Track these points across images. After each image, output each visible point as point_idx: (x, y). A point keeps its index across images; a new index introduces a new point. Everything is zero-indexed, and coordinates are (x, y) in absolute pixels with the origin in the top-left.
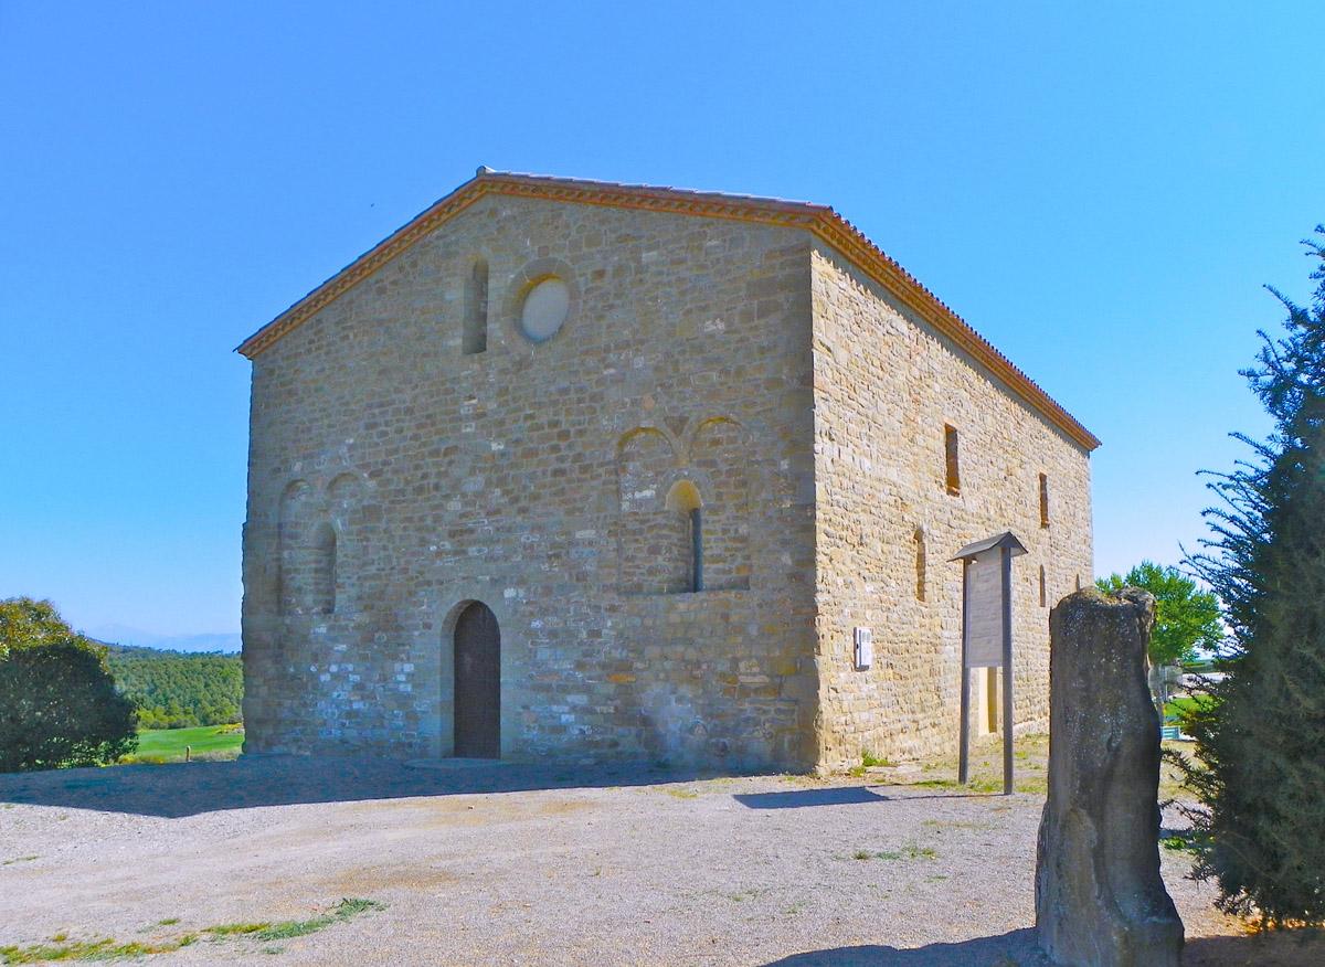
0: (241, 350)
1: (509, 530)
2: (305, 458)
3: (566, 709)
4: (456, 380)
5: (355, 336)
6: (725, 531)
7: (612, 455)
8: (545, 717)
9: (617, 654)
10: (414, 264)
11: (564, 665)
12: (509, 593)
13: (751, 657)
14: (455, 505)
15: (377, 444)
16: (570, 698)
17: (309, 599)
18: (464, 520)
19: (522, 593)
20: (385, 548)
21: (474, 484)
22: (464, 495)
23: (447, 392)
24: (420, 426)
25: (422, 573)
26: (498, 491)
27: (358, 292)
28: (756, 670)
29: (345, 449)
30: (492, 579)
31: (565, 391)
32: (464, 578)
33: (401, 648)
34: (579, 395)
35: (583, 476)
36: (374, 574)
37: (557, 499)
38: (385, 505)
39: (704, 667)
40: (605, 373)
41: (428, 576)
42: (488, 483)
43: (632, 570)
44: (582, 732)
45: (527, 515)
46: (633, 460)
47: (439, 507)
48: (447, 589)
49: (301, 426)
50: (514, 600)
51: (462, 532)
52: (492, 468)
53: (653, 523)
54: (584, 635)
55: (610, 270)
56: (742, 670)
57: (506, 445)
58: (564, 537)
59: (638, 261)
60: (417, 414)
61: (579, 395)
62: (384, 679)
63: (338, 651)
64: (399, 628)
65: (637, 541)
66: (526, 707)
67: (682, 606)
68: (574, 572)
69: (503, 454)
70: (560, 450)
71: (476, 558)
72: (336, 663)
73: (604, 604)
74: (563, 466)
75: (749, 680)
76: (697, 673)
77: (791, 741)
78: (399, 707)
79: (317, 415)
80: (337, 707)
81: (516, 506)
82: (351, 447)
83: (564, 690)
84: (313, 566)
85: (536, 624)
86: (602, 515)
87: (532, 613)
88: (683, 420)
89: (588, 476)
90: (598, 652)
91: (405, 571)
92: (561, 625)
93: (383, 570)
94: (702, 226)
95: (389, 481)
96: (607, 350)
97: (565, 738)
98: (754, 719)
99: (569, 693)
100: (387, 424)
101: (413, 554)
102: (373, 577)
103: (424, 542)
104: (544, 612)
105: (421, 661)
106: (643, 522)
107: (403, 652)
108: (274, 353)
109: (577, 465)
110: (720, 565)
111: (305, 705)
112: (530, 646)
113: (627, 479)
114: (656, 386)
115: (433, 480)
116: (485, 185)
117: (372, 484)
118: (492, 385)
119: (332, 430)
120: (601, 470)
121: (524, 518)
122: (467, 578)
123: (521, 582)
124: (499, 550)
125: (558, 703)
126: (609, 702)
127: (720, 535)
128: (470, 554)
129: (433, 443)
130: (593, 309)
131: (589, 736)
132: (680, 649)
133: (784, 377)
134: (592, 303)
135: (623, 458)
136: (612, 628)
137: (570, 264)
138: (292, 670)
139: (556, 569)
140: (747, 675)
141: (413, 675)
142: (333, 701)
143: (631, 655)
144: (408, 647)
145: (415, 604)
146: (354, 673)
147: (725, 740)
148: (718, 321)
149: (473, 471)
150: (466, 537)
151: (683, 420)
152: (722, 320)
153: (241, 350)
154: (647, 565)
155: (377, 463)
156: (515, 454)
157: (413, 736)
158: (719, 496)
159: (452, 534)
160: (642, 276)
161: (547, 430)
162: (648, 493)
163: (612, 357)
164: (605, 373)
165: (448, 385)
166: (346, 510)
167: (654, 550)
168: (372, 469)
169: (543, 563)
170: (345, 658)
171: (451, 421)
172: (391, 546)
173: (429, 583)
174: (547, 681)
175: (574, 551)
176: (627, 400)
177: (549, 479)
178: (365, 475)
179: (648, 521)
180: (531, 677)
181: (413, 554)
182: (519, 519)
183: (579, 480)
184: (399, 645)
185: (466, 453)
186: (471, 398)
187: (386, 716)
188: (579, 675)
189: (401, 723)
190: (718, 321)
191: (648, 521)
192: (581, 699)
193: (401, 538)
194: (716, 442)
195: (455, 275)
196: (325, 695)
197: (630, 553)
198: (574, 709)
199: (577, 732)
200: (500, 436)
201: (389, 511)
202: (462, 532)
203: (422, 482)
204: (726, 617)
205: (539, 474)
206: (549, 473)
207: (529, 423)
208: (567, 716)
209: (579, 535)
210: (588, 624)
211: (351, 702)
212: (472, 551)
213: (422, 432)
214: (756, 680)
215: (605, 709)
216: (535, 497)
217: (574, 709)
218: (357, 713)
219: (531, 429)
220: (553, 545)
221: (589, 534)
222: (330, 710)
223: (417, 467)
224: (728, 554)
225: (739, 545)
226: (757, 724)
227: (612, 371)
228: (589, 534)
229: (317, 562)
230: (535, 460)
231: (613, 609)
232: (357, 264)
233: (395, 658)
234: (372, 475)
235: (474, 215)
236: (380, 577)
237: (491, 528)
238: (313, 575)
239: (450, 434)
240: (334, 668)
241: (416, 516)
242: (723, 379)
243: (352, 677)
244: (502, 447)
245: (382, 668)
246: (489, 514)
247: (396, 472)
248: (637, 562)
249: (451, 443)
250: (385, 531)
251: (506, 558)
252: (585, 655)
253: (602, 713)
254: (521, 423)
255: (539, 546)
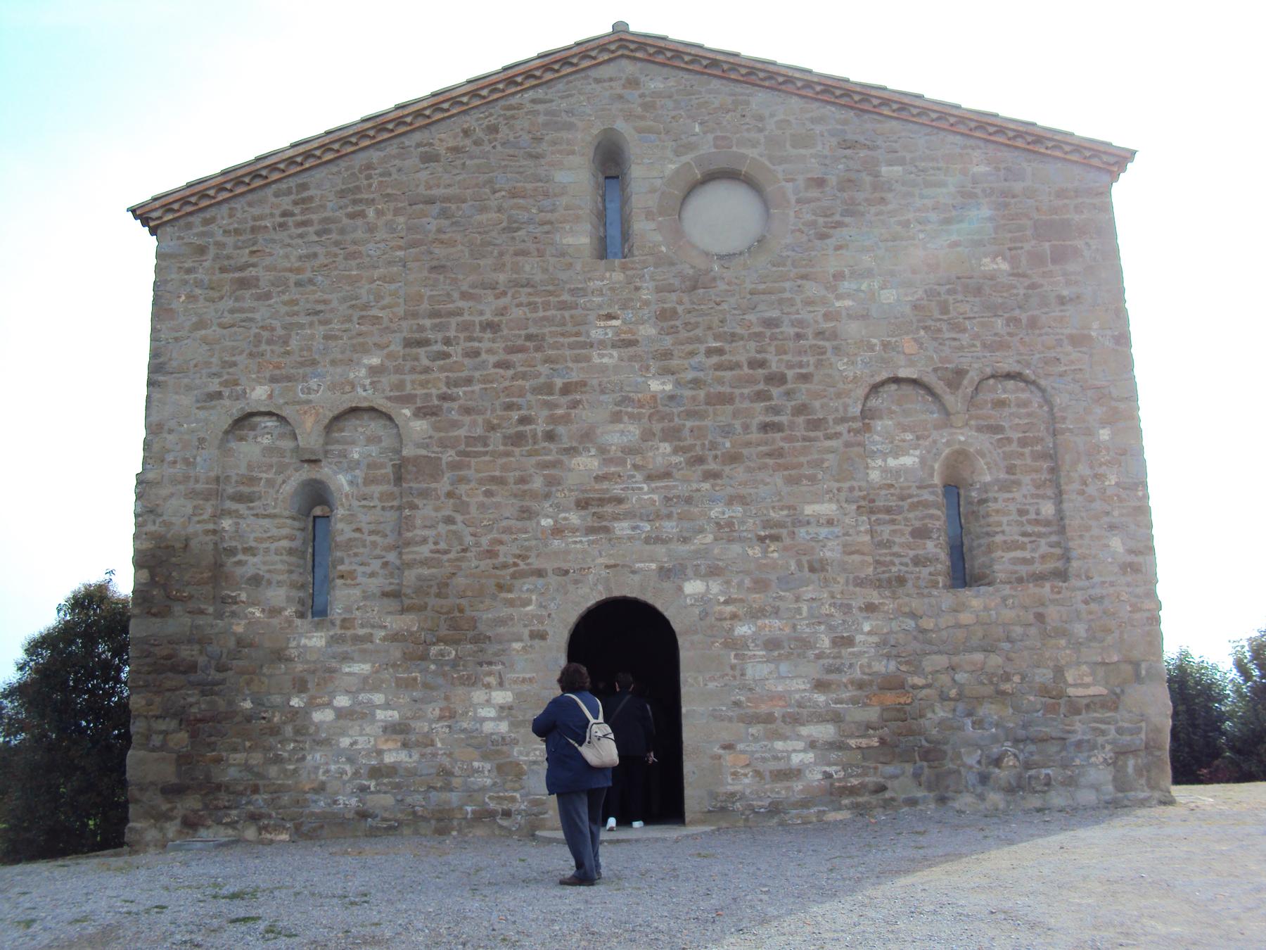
0: (142, 214)
1: (689, 500)
2: (273, 380)
3: (800, 745)
4: (582, 292)
5: (380, 213)
6: (1021, 512)
7: (856, 410)
8: (764, 760)
9: (880, 667)
10: (493, 129)
11: (792, 683)
12: (693, 587)
13: (1078, 664)
14: (587, 463)
15: (427, 370)
16: (804, 731)
17: (277, 595)
18: (605, 485)
19: (715, 587)
20: (449, 520)
21: (618, 436)
22: (602, 450)
23: (563, 306)
24: (512, 350)
25: (523, 557)
26: (666, 447)
27: (382, 154)
28: (1088, 680)
29: (363, 372)
30: (661, 568)
31: (770, 323)
32: (607, 567)
33: (486, 668)
34: (797, 330)
35: (812, 434)
36: (426, 559)
37: (770, 461)
38: (449, 456)
39: (1016, 679)
40: (837, 304)
41: (536, 563)
42: (647, 435)
43: (888, 559)
44: (828, 776)
45: (719, 482)
46: (881, 418)
47: (553, 465)
48: (576, 582)
49: (266, 334)
50: (702, 599)
51: (602, 502)
52: (650, 416)
53: (915, 500)
54: (825, 643)
55: (833, 180)
56: (1070, 680)
57: (678, 384)
58: (785, 512)
59: (877, 175)
60: (505, 332)
61: (797, 330)
62: (449, 715)
63: (349, 674)
64: (480, 639)
65: (893, 522)
66: (729, 747)
67: (976, 603)
68: (805, 559)
69: (672, 398)
70: (770, 398)
71: (630, 538)
72: (347, 692)
73: (856, 603)
74: (776, 419)
75: (1080, 692)
76: (1007, 687)
77: (1135, 766)
78: (485, 757)
79: (303, 320)
80: (350, 760)
81: (700, 469)
82: (373, 371)
83: (795, 720)
84: (285, 543)
85: (743, 630)
86: (846, 485)
87: (734, 616)
88: (960, 373)
89: (820, 434)
90: (851, 665)
91: (491, 554)
92: (787, 630)
93: (446, 552)
94: (965, 147)
95: (455, 425)
96: (839, 276)
97: (798, 786)
98: (1088, 741)
99: (803, 725)
100: (447, 342)
101: (507, 530)
102: (424, 563)
103: (527, 514)
104: (756, 614)
105: (525, 687)
106: (903, 498)
107: (490, 674)
108: (877, 214)
109: (801, 420)
110: (1019, 554)
111: (278, 760)
112: (734, 661)
113: (876, 440)
114: (918, 329)
115: (540, 427)
116: (623, 46)
117: (420, 426)
118: (647, 303)
119: (332, 343)
120: (839, 428)
121: (713, 486)
122: (615, 566)
123: (713, 572)
124: (670, 527)
125: (784, 738)
126: (871, 732)
127: (1015, 516)
128: (618, 532)
129: (539, 375)
130: (813, 224)
131: (839, 780)
132: (978, 657)
133: (1094, 334)
134: (809, 217)
135: (867, 415)
136: (870, 633)
137: (767, 163)
138: (248, 705)
139: (776, 555)
140: (1075, 685)
141: (510, 708)
142: (340, 753)
143: (903, 668)
144: (500, 667)
145: (511, 603)
146: (387, 706)
147: (1049, 771)
148: (999, 259)
149: (616, 418)
150: (609, 509)
151: (960, 373)
152: (1004, 259)
153: (142, 214)
154: (912, 553)
155: (428, 396)
156: (694, 398)
157: (513, 799)
158: (1010, 470)
159: (582, 504)
160: (883, 195)
161: (746, 370)
162: (909, 461)
163: (846, 286)
164: (837, 304)
165: (566, 297)
166: (358, 463)
167: (921, 533)
168: (419, 404)
169: (752, 547)
170: (367, 684)
171: (572, 346)
172: (459, 518)
173: (540, 573)
174: (764, 709)
175: (803, 530)
176: (874, 341)
177: (755, 436)
178: (407, 412)
179: (910, 496)
180: (737, 704)
181: (507, 530)
182: (706, 486)
183: (805, 439)
184: (481, 664)
185: (603, 392)
186: (610, 317)
187: (457, 771)
188: (820, 698)
189: (489, 782)
190: (999, 259)
191: (910, 496)
192: (826, 732)
193: (482, 506)
194: (1001, 404)
195: (573, 153)
196: (326, 742)
197: (886, 536)
198: (812, 745)
199: (820, 776)
200: (666, 371)
201: (454, 466)
202: (602, 502)
203: (521, 428)
204: (1040, 617)
205: (739, 429)
206: (754, 428)
207: (715, 359)
208: (801, 756)
209: (809, 510)
210: (831, 628)
211: (380, 752)
212: (622, 528)
213: (516, 358)
214: (1092, 691)
215: (864, 742)
216: (734, 458)
217: (812, 745)
218: (392, 770)
219: (719, 367)
220: (767, 524)
221: (827, 508)
222: (333, 767)
223: (509, 407)
224: (1026, 540)
225: (1043, 530)
226: (1094, 747)
227: (848, 303)
228: (827, 508)
229: (291, 538)
230: (729, 408)
231: (870, 608)
232: (392, 116)
233: (472, 682)
234: (420, 413)
235: (598, 81)
236: (439, 564)
237: (656, 497)
238: (285, 558)
239: (570, 365)
240: (342, 701)
241: (511, 476)
242: (1012, 329)
243: (380, 715)
244: (669, 387)
245: (447, 698)
246: (649, 478)
247: (467, 411)
248: (896, 549)
249: (575, 377)
250: (450, 495)
251: (685, 540)
252: (829, 670)
253: (859, 748)
254: (701, 358)
255: (743, 523)
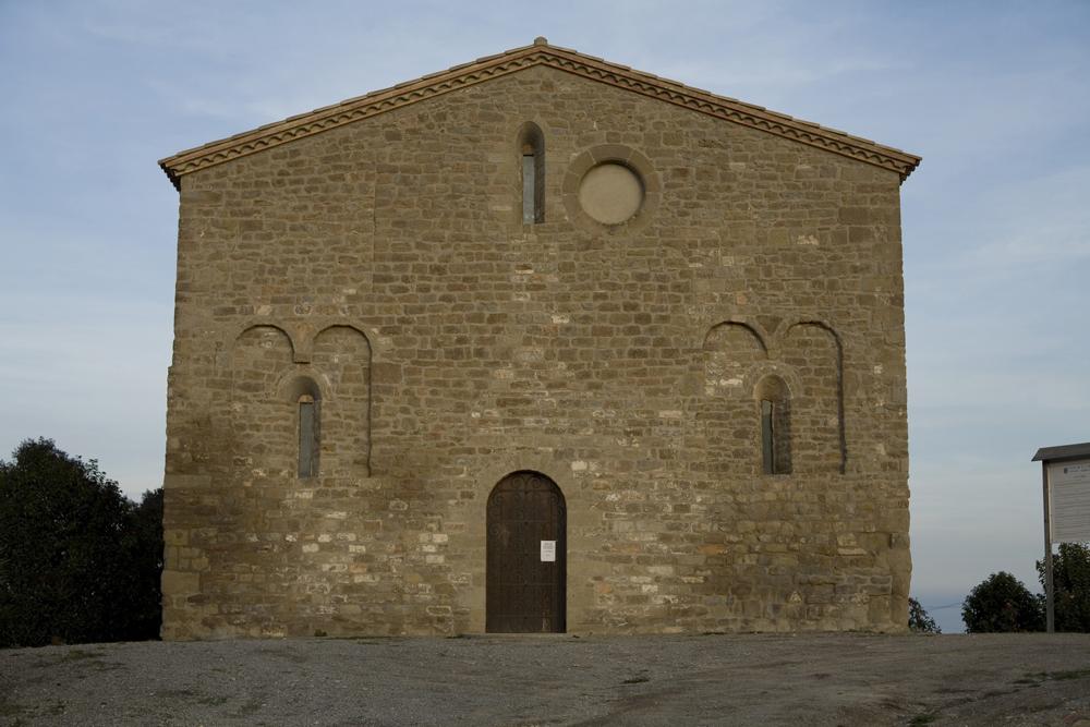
1: (577, 404)
2: (274, 301)
3: (649, 579)
5: (356, 178)
6: (814, 423)
8: (623, 588)
9: (706, 527)
12: (578, 466)
14: (506, 374)
15: (391, 300)
16: (652, 570)
18: (518, 390)
19: (593, 467)
20: (405, 410)
21: (530, 355)
23: (492, 257)
24: (452, 288)
26: (563, 365)
27: (357, 131)
28: (853, 543)
29: (343, 299)
30: (556, 451)
31: (641, 277)
34: (661, 283)
35: (667, 360)
37: (637, 379)
38: (406, 363)
39: (803, 540)
40: (691, 266)
41: (468, 445)
42: (549, 355)
45: (599, 391)
47: (483, 373)
49: (268, 266)
50: (584, 474)
51: (516, 402)
52: (553, 342)
54: (670, 508)
56: (841, 543)
57: (573, 319)
59: (725, 168)
60: (449, 274)
61: (661, 283)
62: (402, 550)
63: (329, 519)
64: (424, 497)
65: (721, 425)
66: (598, 578)
67: (777, 486)
69: (568, 329)
70: (639, 333)
71: (535, 429)
72: (328, 532)
74: (642, 348)
78: (426, 580)
79: (298, 256)
80: (330, 580)
81: (587, 381)
82: (350, 298)
83: (646, 561)
85: (612, 497)
87: (606, 487)
88: (776, 320)
90: (687, 526)
91: (436, 436)
92: (643, 498)
93: (402, 434)
95: (410, 341)
96: (693, 245)
97: (647, 608)
99: (651, 565)
102: (387, 440)
105: (457, 532)
106: (729, 409)
107: (432, 522)
109: (659, 349)
110: (810, 452)
112: (605, 519)
113: (712, 366)
115: (473, 346)
116: (544, 56)
117: (384, 342)
118: (553, 258)
120: (687, 357)
121: (595, 394)
122: (523, 448)
123: (592, 456)
124: (563, 423)
125: (638, 574)
126: (698, 572)
127: (809, 426)
129: (472, 307)
131: (675, 605)
132: (777, 524)
133: (876, 295)
134: (674, 199)
136: (701, 503)
139: (637, 445)
140: (844, 547)
141: (446, 546)
142: (322, 575)
144: (440, 517)
145: (449, 472)
146: (357, 543)
148: (811, 237)
149: (527, 342)
150: (521, 407)
151: (776, 320)
154: (733, 448)
157: (447, 611)
158: (808, 392)
159: (501, 403)
160: (730, 184)
162: (735, 382)
163: (698, 252)
164: (691, 266)
165: (493, 250)
167: (741, 434)
170: (343, 526)
171: (497, 287)
172: (412, 410)
173: (470, 451)
174: (625, 553)
175: (657, 428)
176: (715, 294)
177: (626, 359)
178: (375, 330)
179: (735, 407)
180: (606, 549)
181: (447, 420)
182: (590, 394)
184: (426, 514)
185: (518, 322)
186: (526, 267)
187: (406, 589)
190: (811, 237)
192: (665, 571)
194: (805, 343)
195: (501, 139)
196: (313, 567)
198: (657, 579)
200: (564, 310)
201: (409, 372)
202: (516, 402)
204: (822, 498)
206: (626, 354)
207: (600, 302)
208: (649, 586)
209: (662, 414)
210: (673, 498)
211: (351, 575)
212: (529, 421)
213: (456, 294)
214: (855, 552)
215: (693, 580)
216: (611, 375)
217: (657, 579)
218: (361, 587)
219: (603, 308)
221: (675, 414)
222: (317, 585)
223: (450, 330)
224: (816, 442)
225: (829, 436)
227: (699, 265)
228: (675, 414)
230: (609, 339)
231: (702, 486)
233: (420, 527)
234: (384, 332)
235: (521, 83)
237: (554, 401)
239: (496, 301)
240: (325, 538)
241: (451, 380)
244: (566, 321)
246: (550, 386)
247: (420, 332)
248: (723, 445)
249: (499, 311)
250: (406, 392)
251: (574, 432)
252: (671, 528)
254: (590, 301)
